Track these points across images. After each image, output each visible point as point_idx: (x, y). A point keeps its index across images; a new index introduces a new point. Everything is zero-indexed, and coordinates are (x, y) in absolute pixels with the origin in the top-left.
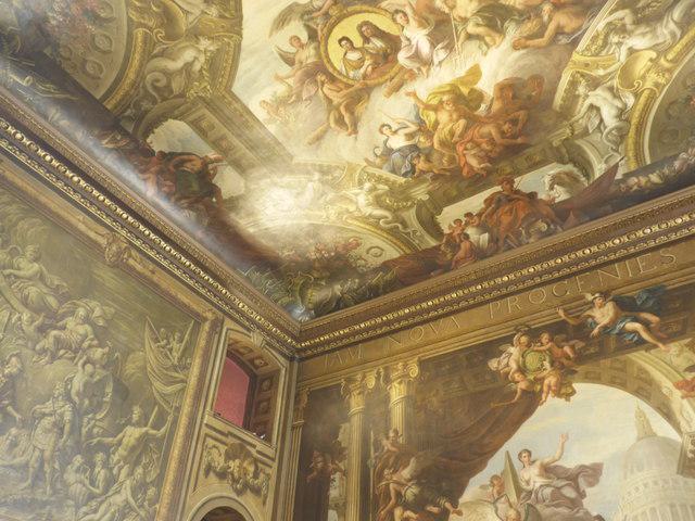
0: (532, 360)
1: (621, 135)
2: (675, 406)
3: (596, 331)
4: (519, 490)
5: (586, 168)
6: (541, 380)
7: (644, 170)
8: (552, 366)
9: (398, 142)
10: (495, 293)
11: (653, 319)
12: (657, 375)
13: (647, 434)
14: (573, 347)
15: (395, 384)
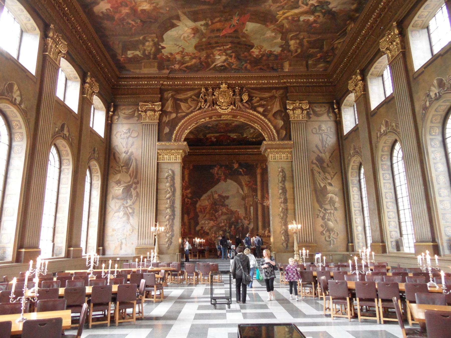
0: (220, 172)
1: (252, 133)
2: (244, 188)
3: (233, 169)
4: (213, 198)
5: (243, 135)
6: (221, 177)
7: (254, 138)
8: (224, 174)
9: (210, 126)
10: (214, 153)
11: (245, 170)
12: (243, 181)
13: (238, 192)
14: (228, 171)
15: (186, 169)
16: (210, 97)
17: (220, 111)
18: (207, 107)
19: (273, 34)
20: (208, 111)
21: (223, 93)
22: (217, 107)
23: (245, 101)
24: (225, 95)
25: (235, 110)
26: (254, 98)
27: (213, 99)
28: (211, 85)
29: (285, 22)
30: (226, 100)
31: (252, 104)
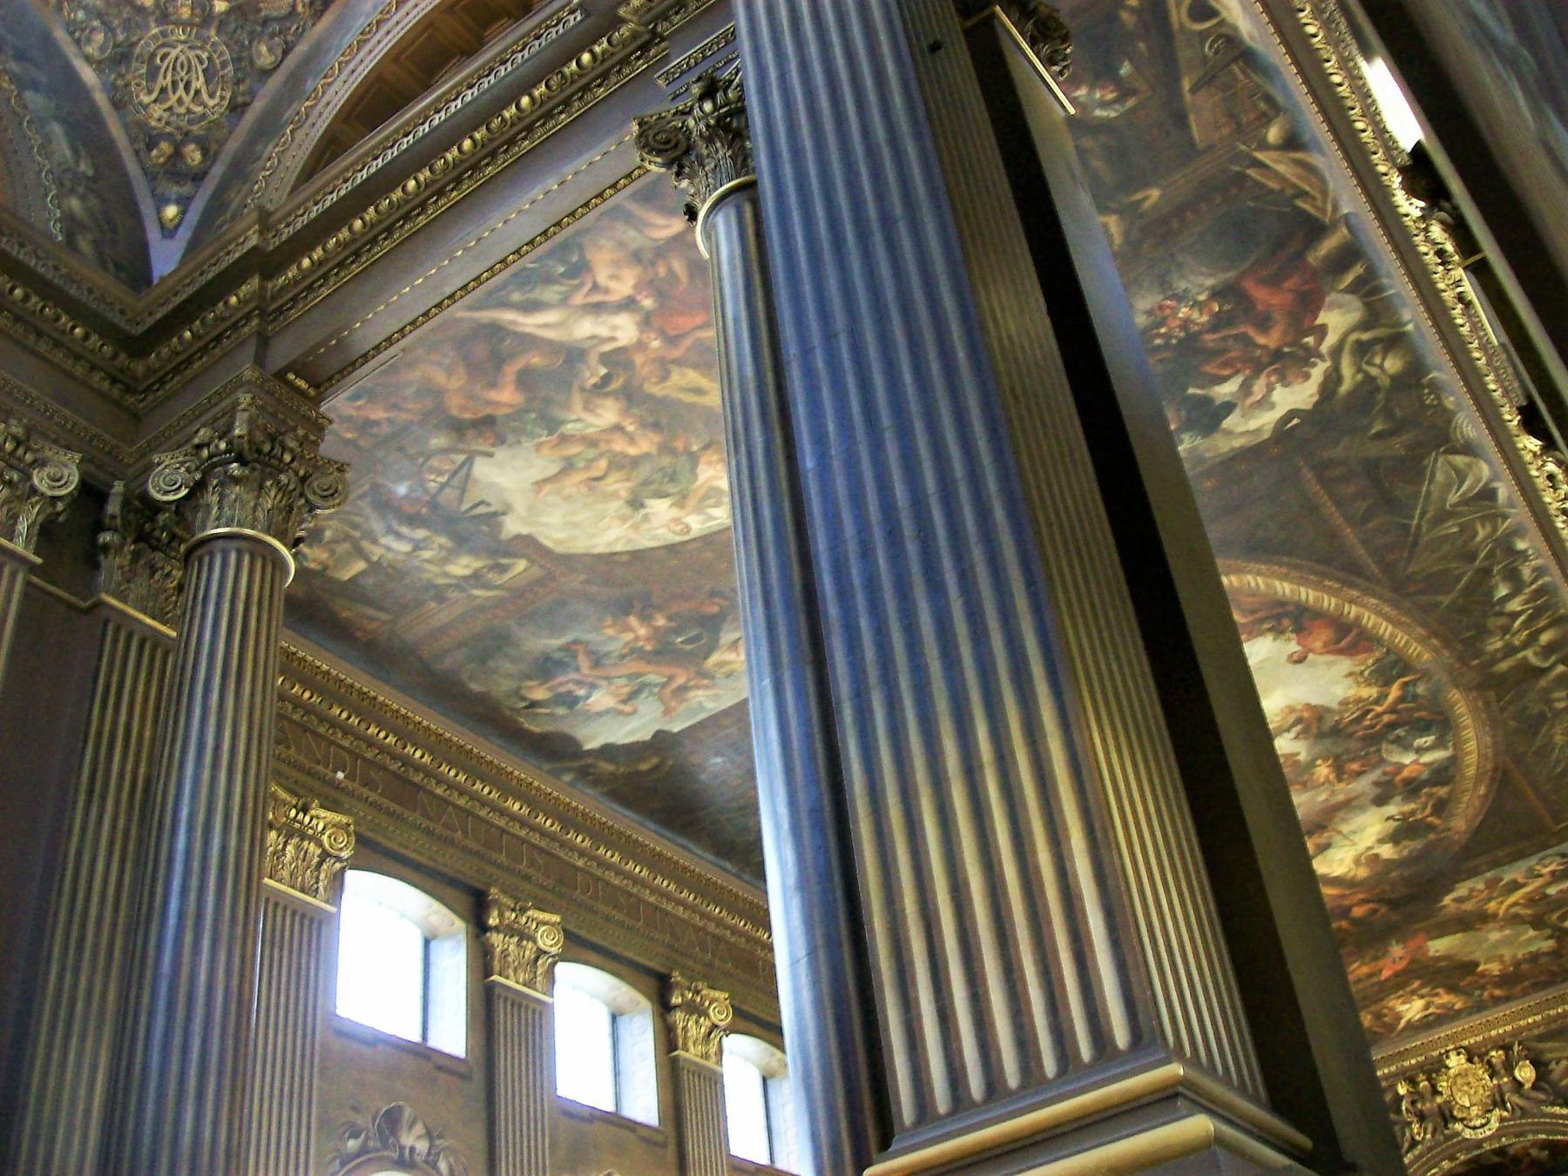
16: (1428, 1105)
17: (1468, 1134)
18: (1429, 1136)
19: (1507, 932)
20: (1438, 1144)
21: (1460, 1081)
22: (1458, 1126)
23: (1528, 1086)
24: (1469, 1084)
25: (1509, 1120)
26: (1553, 1066)
27: (1439, 1106)
28: (1420, 1067)
29: (1513, 910)
30: (1474, 1100)
31: (1554, 1085)
